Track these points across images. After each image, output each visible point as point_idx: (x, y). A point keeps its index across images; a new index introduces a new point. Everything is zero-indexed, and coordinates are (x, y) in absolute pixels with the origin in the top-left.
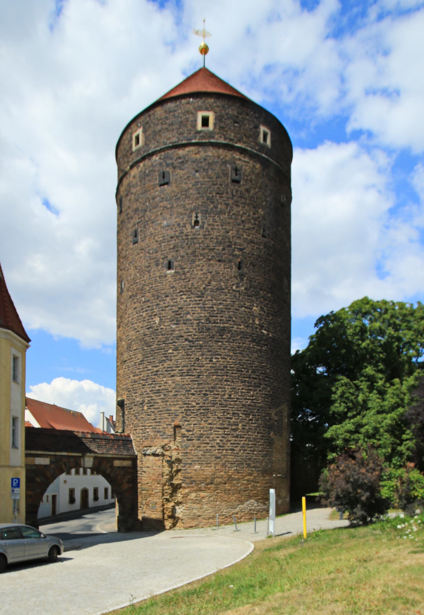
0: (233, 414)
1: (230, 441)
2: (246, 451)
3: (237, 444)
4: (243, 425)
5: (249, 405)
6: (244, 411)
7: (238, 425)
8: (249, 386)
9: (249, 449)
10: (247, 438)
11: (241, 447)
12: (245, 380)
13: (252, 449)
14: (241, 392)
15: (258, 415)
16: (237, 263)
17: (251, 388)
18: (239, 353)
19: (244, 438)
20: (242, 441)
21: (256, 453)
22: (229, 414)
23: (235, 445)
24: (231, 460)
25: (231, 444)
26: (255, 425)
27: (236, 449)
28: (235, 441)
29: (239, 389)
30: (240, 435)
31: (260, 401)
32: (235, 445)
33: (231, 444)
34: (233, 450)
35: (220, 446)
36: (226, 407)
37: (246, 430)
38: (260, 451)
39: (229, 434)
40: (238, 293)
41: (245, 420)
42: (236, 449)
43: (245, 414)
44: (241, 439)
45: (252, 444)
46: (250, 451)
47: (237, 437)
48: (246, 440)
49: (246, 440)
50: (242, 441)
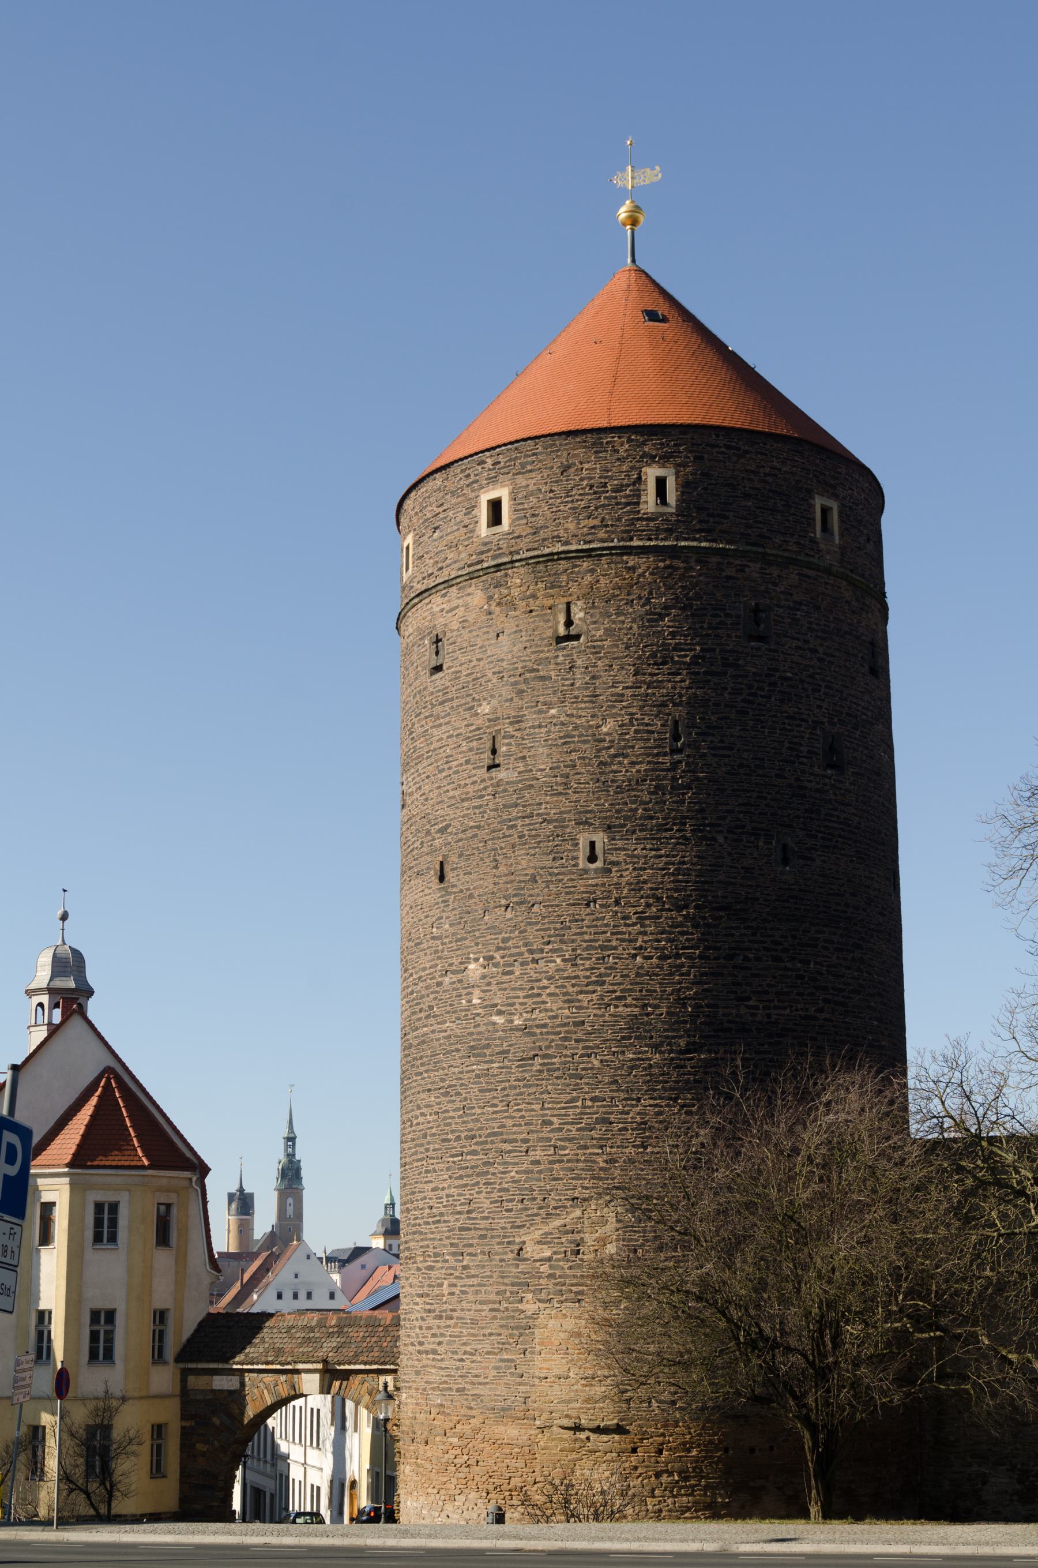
0: (436, 1255)
1: (429, 1328)
2: (456, 1353)
3: (442, 1335)
4: (450, 1285)
5: (461, 1229)
6: (452, 1245)
7: (441, 1285)
8: (461, 1177)
9: (464, 1348)
10: (458, 1318)
11: (449, 1343)
12: (454, 1162)
13: (468, 1349)
14: (448, 1196)
15: (483, 1253)
16: (438, 867)
17: (464, 1181)
18: (442, 1094)
19: (451, 1318)
20: (449, 1326)
21: (479, 1358)
22: (429, 1256)
23: (437, 1340)
24: (432, 1378)
25: (434, 1335)
26: (475, 1281)
27: (439, 1348)
28: (439, 1327)
29: (443, 1189)
30: (445, 1311)
31: (486, 1214)
32: (437, 1340)
33: (434, 1335)
34: (434, 1352)
35: (421, 1344)
36: (426, 1240)
37: (455, 1299)
38: (488, 1353)
39: (429, 1311)
40: (439, 942)
41: (455, 1268)
42: (439, 1348)
43: (454, 1254)
44: (449, 1322)
45: (470, 1334)
46: (465, 1353)
47: (440, 1317)
48: (455, 1326)
49: (455, 1326)
50: (449, 1326)
